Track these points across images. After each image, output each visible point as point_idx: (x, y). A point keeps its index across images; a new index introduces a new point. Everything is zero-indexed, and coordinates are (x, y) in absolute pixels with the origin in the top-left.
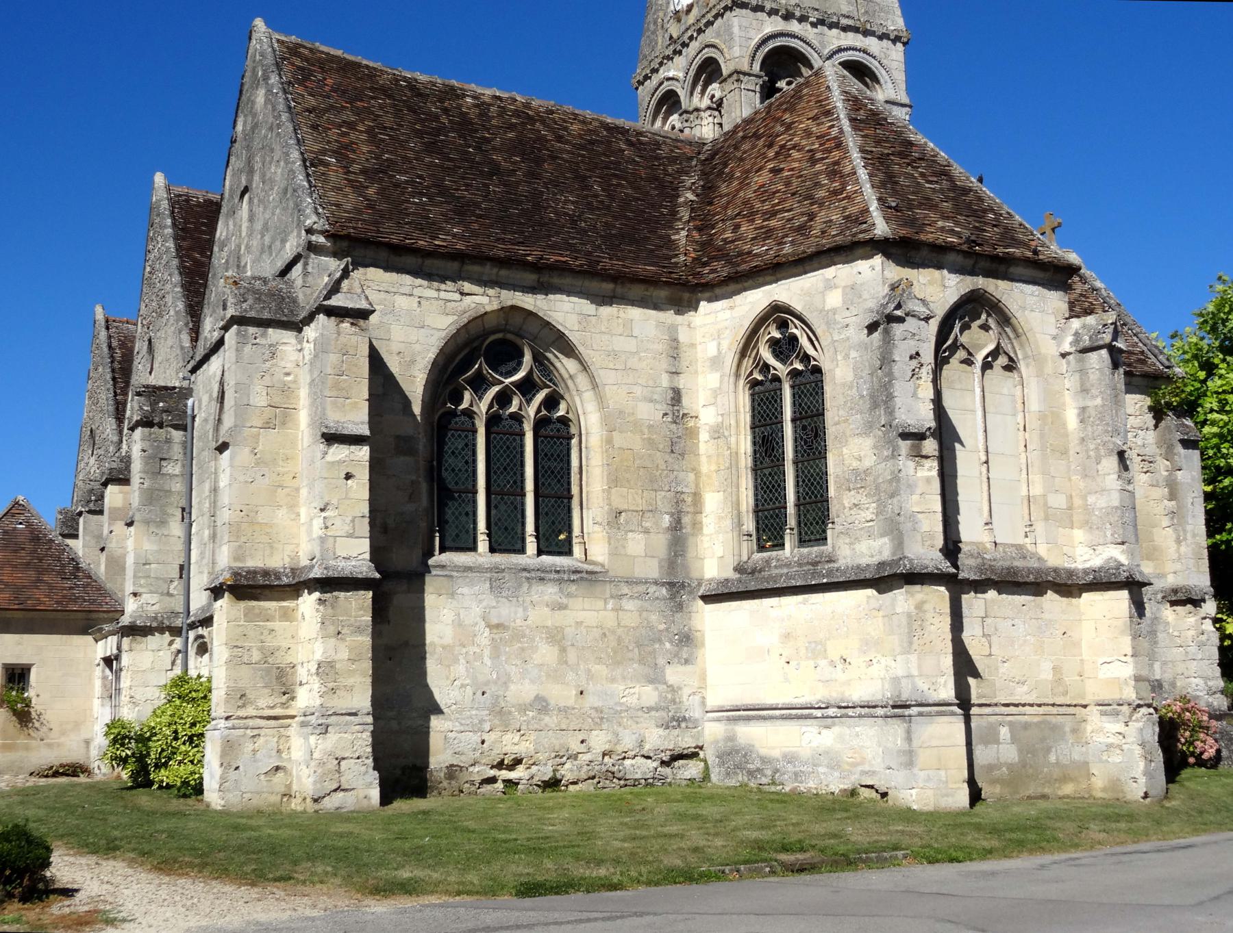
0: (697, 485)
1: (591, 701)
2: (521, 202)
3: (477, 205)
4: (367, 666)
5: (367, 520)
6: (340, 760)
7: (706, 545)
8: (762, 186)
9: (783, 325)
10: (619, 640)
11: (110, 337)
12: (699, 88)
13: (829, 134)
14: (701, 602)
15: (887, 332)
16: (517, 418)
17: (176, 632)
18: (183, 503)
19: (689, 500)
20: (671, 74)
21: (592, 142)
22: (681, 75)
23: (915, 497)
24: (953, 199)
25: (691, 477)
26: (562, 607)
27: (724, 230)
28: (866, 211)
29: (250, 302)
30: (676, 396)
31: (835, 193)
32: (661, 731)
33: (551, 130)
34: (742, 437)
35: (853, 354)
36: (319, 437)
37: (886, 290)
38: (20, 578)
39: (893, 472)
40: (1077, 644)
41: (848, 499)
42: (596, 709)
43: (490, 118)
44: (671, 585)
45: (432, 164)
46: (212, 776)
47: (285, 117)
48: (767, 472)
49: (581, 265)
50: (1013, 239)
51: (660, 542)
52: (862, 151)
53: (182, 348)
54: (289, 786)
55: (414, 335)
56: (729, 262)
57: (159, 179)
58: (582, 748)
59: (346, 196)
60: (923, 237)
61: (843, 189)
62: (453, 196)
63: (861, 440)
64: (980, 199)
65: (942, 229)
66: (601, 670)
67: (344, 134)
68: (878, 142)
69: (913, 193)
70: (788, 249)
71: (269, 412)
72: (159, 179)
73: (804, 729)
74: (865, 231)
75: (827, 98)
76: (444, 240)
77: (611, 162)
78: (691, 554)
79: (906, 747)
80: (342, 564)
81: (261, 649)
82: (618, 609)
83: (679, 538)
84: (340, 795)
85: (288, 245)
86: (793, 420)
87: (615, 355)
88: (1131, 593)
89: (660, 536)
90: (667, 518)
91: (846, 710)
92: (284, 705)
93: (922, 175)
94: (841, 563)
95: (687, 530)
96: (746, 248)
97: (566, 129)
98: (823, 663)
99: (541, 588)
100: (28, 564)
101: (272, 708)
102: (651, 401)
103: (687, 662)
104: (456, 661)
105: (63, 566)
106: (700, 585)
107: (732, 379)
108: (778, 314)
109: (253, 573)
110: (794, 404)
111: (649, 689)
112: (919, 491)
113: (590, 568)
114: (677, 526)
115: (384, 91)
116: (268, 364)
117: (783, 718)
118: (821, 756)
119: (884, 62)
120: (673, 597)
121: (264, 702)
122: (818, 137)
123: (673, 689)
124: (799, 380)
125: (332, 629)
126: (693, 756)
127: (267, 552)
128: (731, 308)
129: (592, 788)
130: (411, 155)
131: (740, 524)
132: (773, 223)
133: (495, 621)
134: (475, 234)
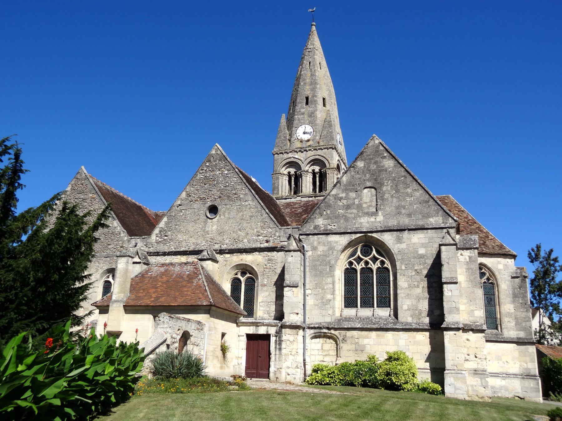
12: (309, 165)
17: (304, 329)
20: (297, 157)
35: (507, 282)
63: (509, 305)
91: (508, 375)
98: (500, 362)
118: (501, 387)
124: (485, 284)
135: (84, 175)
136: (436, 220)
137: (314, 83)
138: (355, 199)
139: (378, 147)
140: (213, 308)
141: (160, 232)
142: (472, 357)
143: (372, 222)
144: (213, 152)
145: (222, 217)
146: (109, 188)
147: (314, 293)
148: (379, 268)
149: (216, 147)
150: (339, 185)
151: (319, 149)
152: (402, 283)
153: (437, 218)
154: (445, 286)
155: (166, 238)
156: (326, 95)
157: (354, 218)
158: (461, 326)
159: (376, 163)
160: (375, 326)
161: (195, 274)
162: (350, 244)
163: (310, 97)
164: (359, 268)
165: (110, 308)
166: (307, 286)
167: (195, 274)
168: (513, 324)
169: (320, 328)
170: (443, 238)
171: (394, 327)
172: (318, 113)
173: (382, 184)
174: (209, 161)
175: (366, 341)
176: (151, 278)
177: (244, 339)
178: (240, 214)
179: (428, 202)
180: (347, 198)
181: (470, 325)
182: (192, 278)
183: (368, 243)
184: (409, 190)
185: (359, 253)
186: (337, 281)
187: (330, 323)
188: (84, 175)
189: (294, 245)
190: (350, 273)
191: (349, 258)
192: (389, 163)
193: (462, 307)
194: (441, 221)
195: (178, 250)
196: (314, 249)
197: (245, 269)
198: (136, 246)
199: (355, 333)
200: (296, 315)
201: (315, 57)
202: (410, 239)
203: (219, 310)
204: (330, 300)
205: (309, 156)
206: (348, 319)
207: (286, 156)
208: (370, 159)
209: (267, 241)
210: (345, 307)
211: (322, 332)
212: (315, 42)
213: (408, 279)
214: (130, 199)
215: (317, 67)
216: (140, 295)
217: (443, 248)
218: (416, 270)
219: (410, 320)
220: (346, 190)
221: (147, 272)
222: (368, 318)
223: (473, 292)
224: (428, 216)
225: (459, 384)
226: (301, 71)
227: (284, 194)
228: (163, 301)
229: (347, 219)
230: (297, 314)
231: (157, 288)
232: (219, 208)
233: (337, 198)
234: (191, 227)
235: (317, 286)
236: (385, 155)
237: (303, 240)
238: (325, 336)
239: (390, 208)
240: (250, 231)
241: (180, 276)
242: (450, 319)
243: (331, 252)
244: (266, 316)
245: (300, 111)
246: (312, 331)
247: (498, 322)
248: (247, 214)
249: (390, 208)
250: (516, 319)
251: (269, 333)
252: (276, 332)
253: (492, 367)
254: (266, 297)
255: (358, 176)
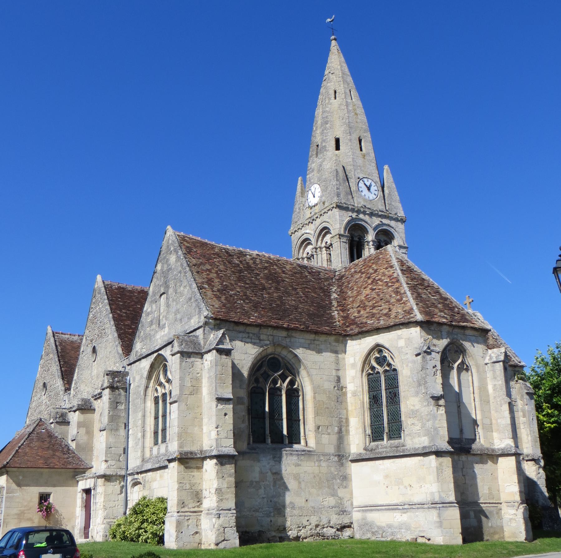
0: (347, 415)
1: (311, 504)
2: (275, 301)
3: (260, 303)
4: (233, 490)
5: (232, 432)
6: (225, 528)
7: (351, 439)
8: (367, 295)
9: (380, 351)
10: (320, 478)
11: (55, 341)
12: (320, 239)
13: (393, 275)
14: (350, 463)
15: (424, 357)
16: (280, 389)
18: (125, 421)
19: (344, 421)
20: (307, 231)
21: (295, 273)
22: (312, 232)
23: (437, 421)
24: (442, 303)
25: (345, 411)
26: (299, 465)
27: (354, 312)
28: (412, 309)
29: (184, 345)
30: (339, 379)
31: (398, 300)
32: (337, 516)
33: (280, 268)
34: (365, 395)
35: (410, 365)
36: (214, 398)
37: (422, 340)
38: (46, 454)
39: (428, 412)
40: (497, 478)
41: (410, 421)
42: (312, 507)
43: (257, 265)
44: (339, 456)
45: (240, 287)
46: (170, 536)
47: (188, 269)
48: (375, 410)
49: (303, 328)
50: (466, 319)
51: (334, 438)
52: (408, 284)
53: (118, 353)
54: (201, 540)
55: (243, 357)
56: (358, 326)
57: (99, 278)
58: (308, 523)
59: (215, 301)
60: (434, 320)
61: (401, 299)
62: (251, 299)
64: (451, 302)
65: (440, 316)
66: (314, 491)
67: (208, 275)
68: (412, 280)
69: (428, 301)
70: (382, 322)
71: (191, 388)
72: (99, 278)
73: (395, 514)
74: (413, 317)
75: (391, 261)
76: (253, 319)
77: (304, 282)
78: (345, 443)
79: (438, 520)
80: (224, 449)
81: (190, 484)
82: (319, 466)
83: (341, 435)
84: (225, 542)
85: (192, 321)
86: (386, 390)
87: (315, 363)
88: (516, 458)
89: (334, 436)
90: (336, 428)
91: (411, 506)
92: (198, 507)
93: (430, 293)
94: (408, 447)
95: (344, 433)
96: (364, 321)
97: (285, 268)
98: (402, 487)
99: (291, 458)
100: (48, 447)
101: (194, 508)
102: (330, 381)
103: (345, 487)
104: (260, 488)
105: (63, 448)
106: (349, 456)
107: (360, 373)
108: (378, 348)
109: (187, 453)
110: (386, 383)
111: (332, 498)
112: (438, 419)
113: (308, 449)
114: (340, 431)
115: (217, 254)
116: (191, 369)
117: (389, 509)
119: (397, 229)
120: (340, 460)
121: (191, 505)
122: (389, 277)
123: (341, 499)
125: (221, 475)
126: (349, 527)
127: (191, 444)
128: (359, 344)
129: (312, 540)
130: (232, 282)
131: (365, 431)
132: (374, 311)
133: (274, 471)
134: (263, 316)
151: (325, 213)
163: (320, 144)
187: (138, 467)
196: (134, 380)
199: (150, 474)
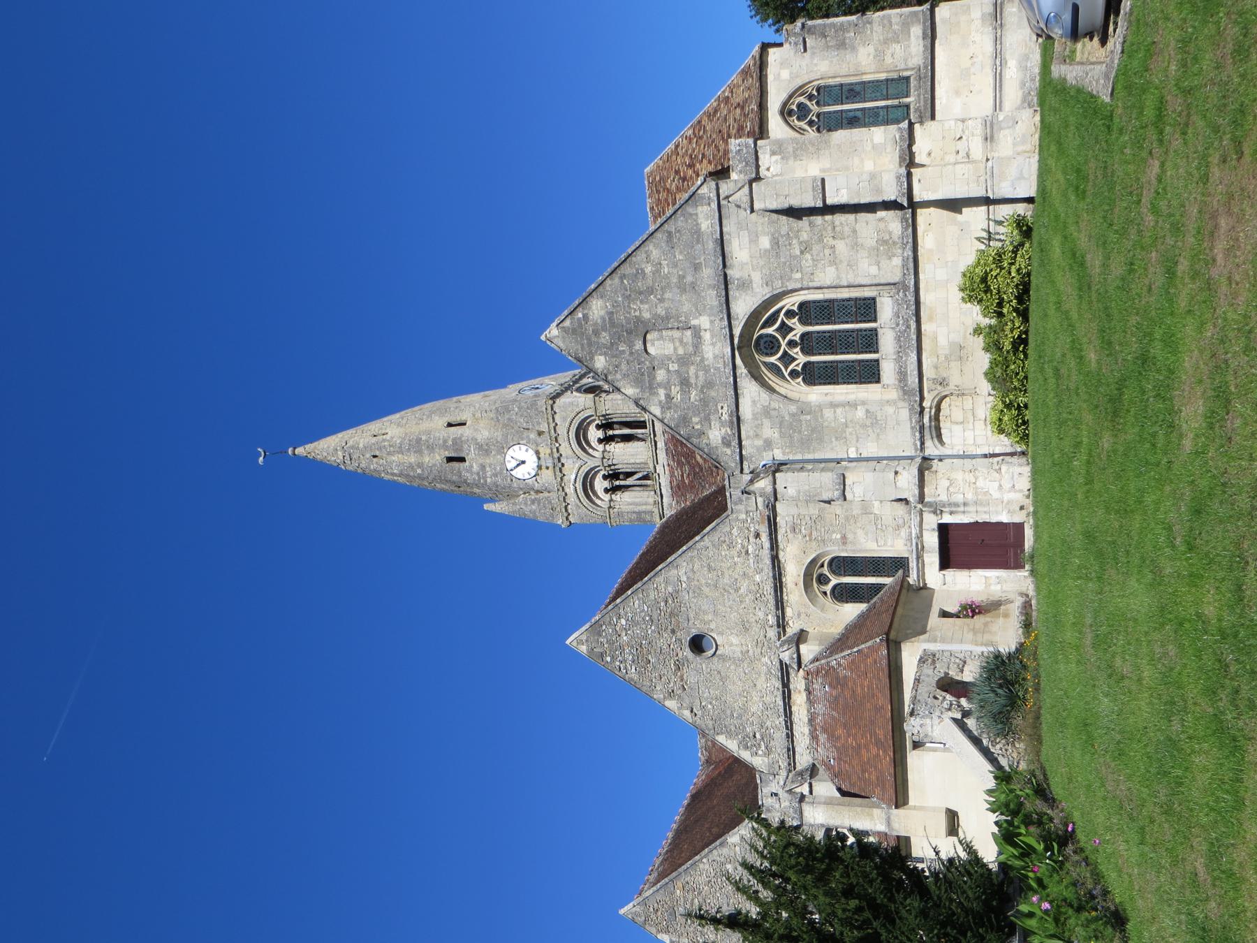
9: (790, 113)
12: (590, 451)
20: (573, 477)
41: (888, 60)
91: (998, 55)
94: (921, 62)
98: (972, 70)
108: (785, 113)
135: (637, 909)
136: (705, 217)
137: (417, 445)
138: (668, 371)
139: (565, 330)
140: (893, 635)
141: (746, 748)
142: (961, 146)
143: (712, 337)
144: (583, 649)
145: (713, 626)
146: (661, 858)
147: (854, 442)
148: (800, 320)
149: (575, 644)
150: (641, 402)
152: (827, 276)
153: (701, 216)
154: (829, 201)
155: (758, 736)
156: (440, 422)
157: (706, 370)
158: (903, 171)
159: (596, 333)
160: (913, 326)
161: (829, 674)
162: (756, 376)
164: (802, 359)
165: (903, 834)
166: (840, 456)
167: (829, 674)
168: (897, 48)
169: (922, 428)
170: (739, 207)
171: (912, 289)
172: (479, 438)
173: (639, 320)
174: (602, 655)
175: (943, 341)
176: (840, 759)
177: (950, 573)
178: (706, 590)
179: (670, 233)
180: (667, 386)
181: (901, 150)
182: (838, 678)
183: (754, 344)
184: (649, 269)
185: (773, 359)
186: (829, 398)
188: (637, 909)
189: (763, 484)
190: (812, 375)
191: (783, 377)
192: (597, 309)
193: (869, 166)
194: (706, 208)
195: (782, 710)
196: (768, 444)
197: (813, 577)
198: (776, 795)
200: (899, 477)
201: (361, 446)
202: (743, 265)
203: (895, 625)
204: (867, 411)
205: (570, 452)
206: (902, 376)
207: (572, 499)
208: (590, 344)
209: (757, 536)
210: (878, 381)
211: (929, 425)
212: (328, 448)
213: (820, 265)
214: (677, 818)
215: (384, 440)
216: (873, 778)
217: (756, 207)
218: (802, 252)
219: (897, 261)
220: (652, 388)
221: (829, 767)
222: (898, 339)
223: (839, 146)
224: (697, 234)
225: (1012, 171)
226: (393, 474)
227: (651, 500)
228: (883, 731)
229: (709, 385)
230: (896, 473)
231: (859, 746)
232: (694, 632)
233: (668, 403)
234: (735, 687)
235: (840, 436)
236: (580, 315)
237: (752, 467)
238: (936, 418)
239: (686, 305)
240: (739, 570)
241: (834, 703)
242: (891, 192)
243: (773, 413)
244: (904, 533)
245: (478, 474)
246: (928, 443)
247: (895, 75)
248: (704, 577)
249: (686, 305)
250: (886, 42)
251: (935, 527)
252: (935, 512)
253: (983, 104)
254: (866, 534)
255: (624, 367)
